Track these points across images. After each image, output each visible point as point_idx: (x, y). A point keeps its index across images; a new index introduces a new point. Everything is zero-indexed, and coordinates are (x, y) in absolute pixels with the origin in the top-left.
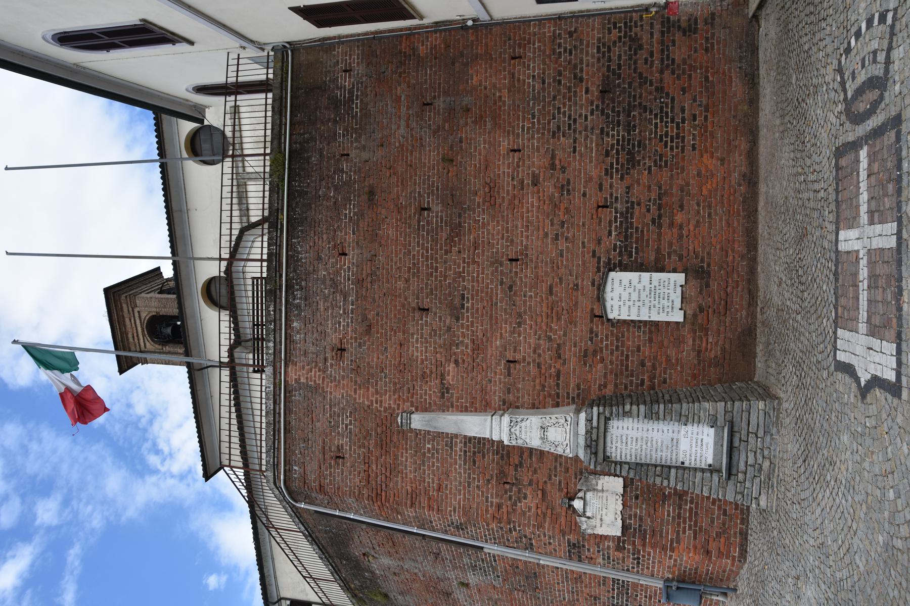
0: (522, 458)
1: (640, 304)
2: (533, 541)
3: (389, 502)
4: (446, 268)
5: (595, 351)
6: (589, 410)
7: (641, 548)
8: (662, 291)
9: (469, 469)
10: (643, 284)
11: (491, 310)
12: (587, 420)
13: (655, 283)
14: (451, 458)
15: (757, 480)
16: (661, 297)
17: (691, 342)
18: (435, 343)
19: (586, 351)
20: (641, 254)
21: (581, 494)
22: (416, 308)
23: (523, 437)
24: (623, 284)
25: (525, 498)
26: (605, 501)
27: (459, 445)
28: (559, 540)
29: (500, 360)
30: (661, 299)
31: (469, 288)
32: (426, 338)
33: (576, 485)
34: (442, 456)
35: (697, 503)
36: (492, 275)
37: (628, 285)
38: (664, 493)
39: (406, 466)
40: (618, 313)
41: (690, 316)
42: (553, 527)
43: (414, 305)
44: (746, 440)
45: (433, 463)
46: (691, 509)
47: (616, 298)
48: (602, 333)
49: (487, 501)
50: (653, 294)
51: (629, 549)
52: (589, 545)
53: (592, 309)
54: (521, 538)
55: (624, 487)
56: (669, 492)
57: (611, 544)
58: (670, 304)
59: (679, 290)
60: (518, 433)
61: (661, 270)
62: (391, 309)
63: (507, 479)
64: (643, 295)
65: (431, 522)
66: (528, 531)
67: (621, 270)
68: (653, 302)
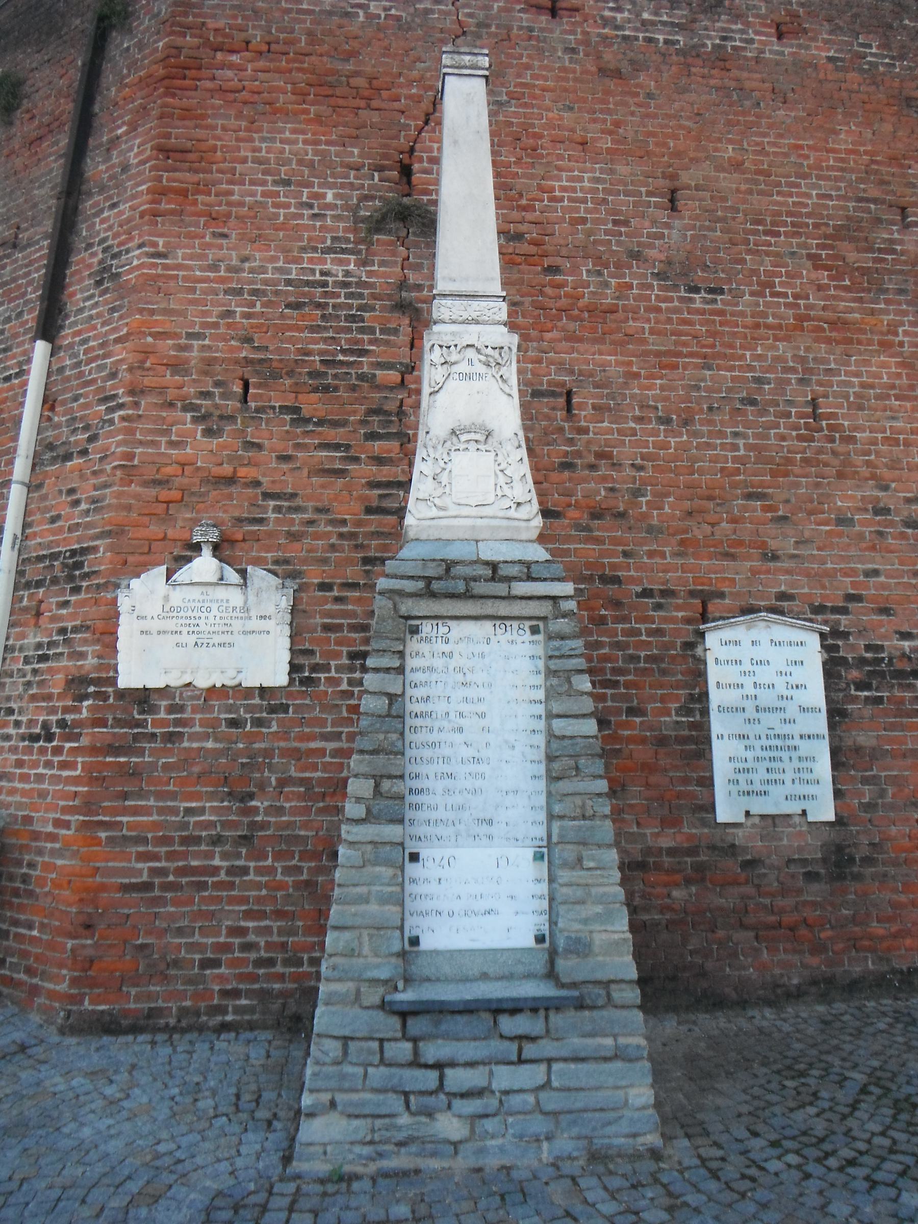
0: (321, 423)
1: (751, 713)
2: (77, 461)
3: (166, 95)
4: (777, 255)
5: (617, 604)
6: (558, 569)
7: (85, 741)
8: (786, 764)
9: (277, 293)
10: (800, 717)
11: (691, 355)
12: (528, 565)
13: (805, 748)
14: (303, 249)
15: (395, 1103)
16: (773, 765)
17: (666, 842)
18: (597, 221)
19: (617, 580)
20: (868, 711)
21: (232, 576)
22: (677, 184)
23: (452, 384)
24: (792, 669)
25: (208, 432)
26: (217, 639)
27: (338, 270)
28: (88, 526)
29: (572, 372)
30: (767, 764)
31: (737, 305)
32: (605, 201)
33: (257, 562)
34: (306, 228)
35: (231, 885)
36: (776, 359)
37: (793, 680)
38: (251, 796)
39: (273, 140)
40: (722, 658)
41: (729, 839)
42: (129, 508)
43: (686, 178)
44: (526, 1055)
45: (287, 206)
46: (215, 870)
47: (759, 653)
48: (665, 620)
49: (190, 336)
50: (778, 743)
51: (77, 710)
52: (83, 603)
53: (722, 595)
54: (87, 428)
55: (262, 690)
56: (257, 808)
57: (91, 661)
58: (757, 787)
59: (794, 808)
60: (463, 367)
61: (836, 764)
62: (667, 126)
63: (259, 386)
64: (771, 720)
65: (114, 206)
66: (114, 443)
67: (824, 664)
68: (758, 744)
